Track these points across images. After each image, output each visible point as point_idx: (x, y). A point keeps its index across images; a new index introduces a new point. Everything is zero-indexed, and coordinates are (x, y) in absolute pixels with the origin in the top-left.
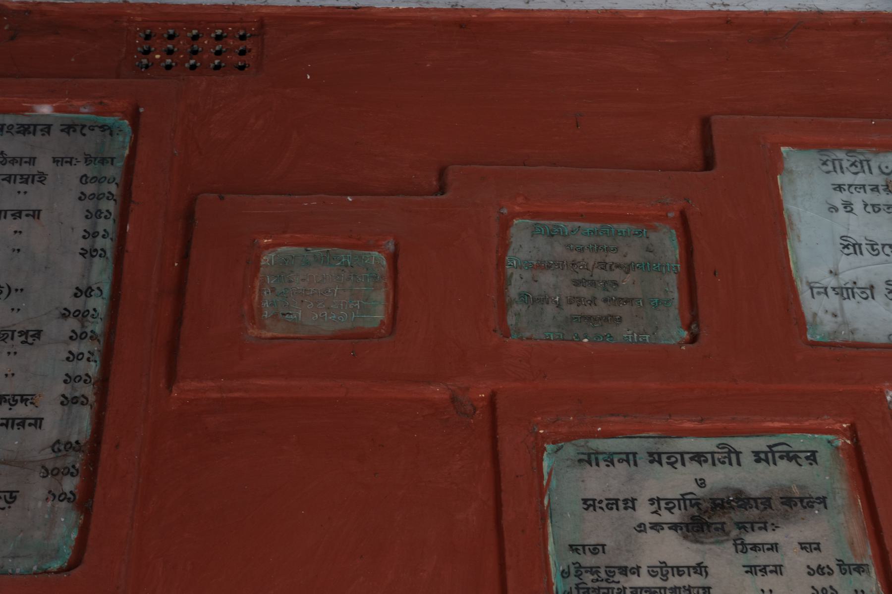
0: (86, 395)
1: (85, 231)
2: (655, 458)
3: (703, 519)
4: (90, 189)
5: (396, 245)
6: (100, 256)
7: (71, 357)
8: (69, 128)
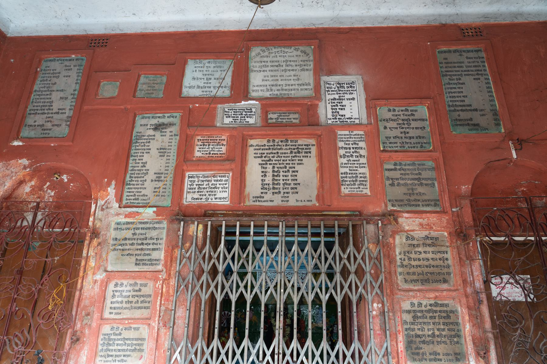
2: (153, 117)
3: (157, 127)
4: (78, 71)
8: (77, 60)
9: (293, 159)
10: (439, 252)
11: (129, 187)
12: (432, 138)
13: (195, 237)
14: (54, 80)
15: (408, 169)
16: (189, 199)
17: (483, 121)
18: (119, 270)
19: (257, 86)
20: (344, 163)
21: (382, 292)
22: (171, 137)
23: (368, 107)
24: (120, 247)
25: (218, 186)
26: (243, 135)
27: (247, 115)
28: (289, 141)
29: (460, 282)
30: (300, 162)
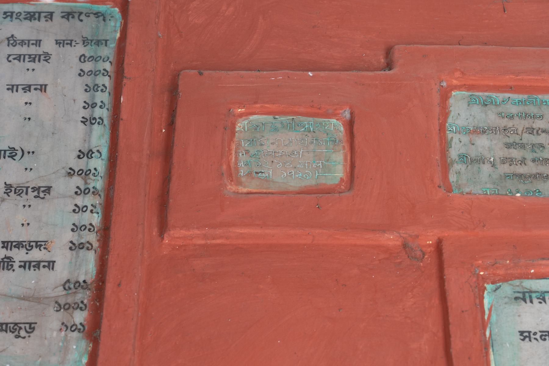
0: (91, 242)
1: (85, 102)
4: (88, 66)
5: (352, 114)
6: (99, 123)
7: (77, 210)
8: (68, 15)
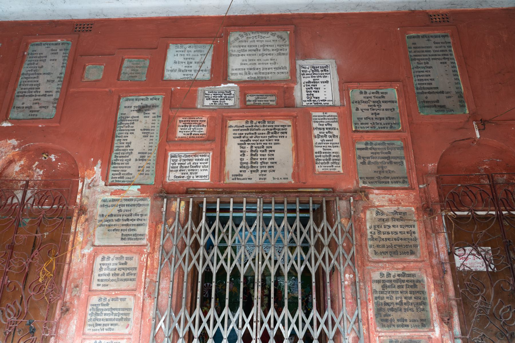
2: (136, 100)
3: (141, 109)
4: (64, 55)
8: (63, 44)
9: (270, 139)
10: (407, 226)
11: (115, 166)
12: (401, 119)
13: (177, 213)
14: (41, 63)
15: (379, 149)
16: (171, 177)
17: (448, 103)
18: (106, 244)
19: (236, 69)
20: (318, 142)
21: (354, 264)
22: (154, 119)
23: (341, 90)
24: (106, 223)
25: (199, 165)
26: (223, 116)
27: (226, 97)
28: (267, 122)
29: (426, 253)
30: (277, 142)
